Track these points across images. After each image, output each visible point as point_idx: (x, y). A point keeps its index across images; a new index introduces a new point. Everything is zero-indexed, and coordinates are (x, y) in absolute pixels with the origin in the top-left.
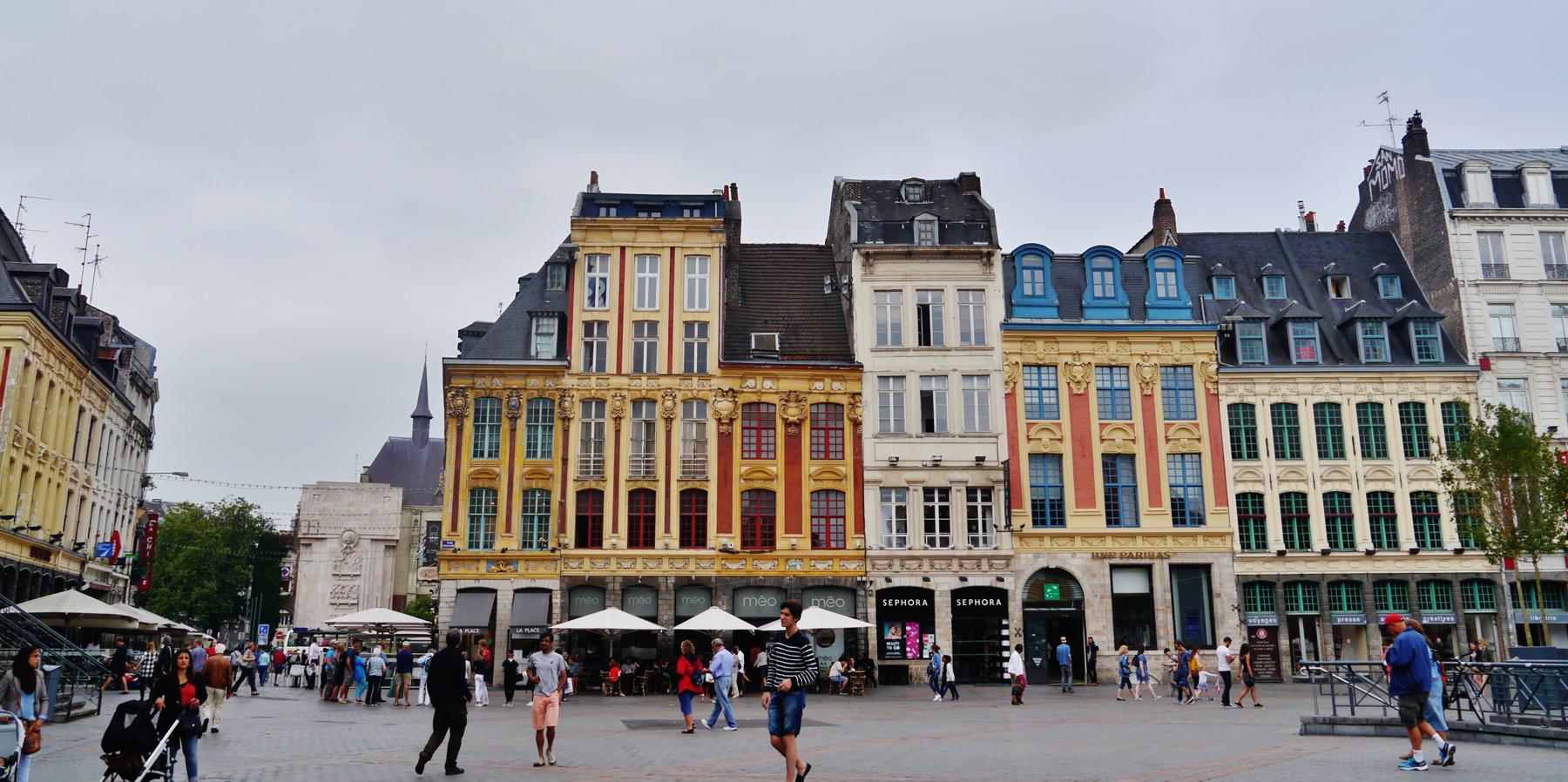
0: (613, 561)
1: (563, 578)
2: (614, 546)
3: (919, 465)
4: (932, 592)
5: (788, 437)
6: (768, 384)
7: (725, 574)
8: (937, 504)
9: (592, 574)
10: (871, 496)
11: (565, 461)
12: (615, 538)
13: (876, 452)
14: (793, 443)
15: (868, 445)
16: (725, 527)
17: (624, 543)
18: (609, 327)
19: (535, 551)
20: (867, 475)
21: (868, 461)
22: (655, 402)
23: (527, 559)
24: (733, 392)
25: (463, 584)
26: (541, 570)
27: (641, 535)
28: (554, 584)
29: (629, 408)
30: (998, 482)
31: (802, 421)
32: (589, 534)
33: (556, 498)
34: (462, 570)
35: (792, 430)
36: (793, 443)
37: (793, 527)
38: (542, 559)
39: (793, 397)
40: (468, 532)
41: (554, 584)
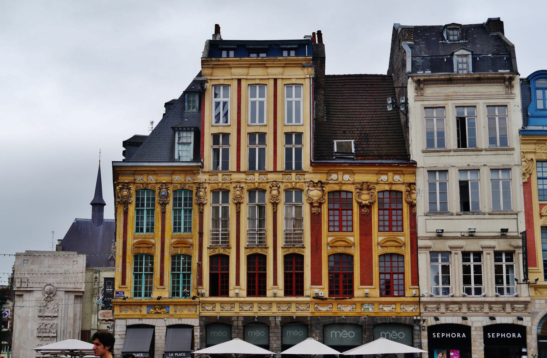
0: (237, 305)
1: (201, 318)
2: (237, 295)
3: (459, 235)
4: (525, 328)
5: (361, 215)
6: (347, 177)
7: (317, 314)
8: (504, 264)
9: (300, 314)
10: (423, 258)
11: (201, 234)
12: (238, 289)
13: (426, 226)
14: (365, 220)
15: (421, 221)
16: (316, 281)
17: (244, 293)
18: (267, 137)
19: (181, 299)
20: (420, 243)
21: (421, 232)
22: (264, 191)
23: (176, 304)
24: (321, 184)
25: (131, 322)
26: (186, 312)
27: (257, 286)
28: (195, 322)
29: (283, 197)
30: (518, 247)
31: (372, 204)
32: (219, 286)
33: (195, 260)
34: (129, 312)
35: (365, 210)
36: (365, 220)
37: (367, 280)
38: (186, 304)
39: (365, 186)
40: (133, 285)
41: (195, 322)
